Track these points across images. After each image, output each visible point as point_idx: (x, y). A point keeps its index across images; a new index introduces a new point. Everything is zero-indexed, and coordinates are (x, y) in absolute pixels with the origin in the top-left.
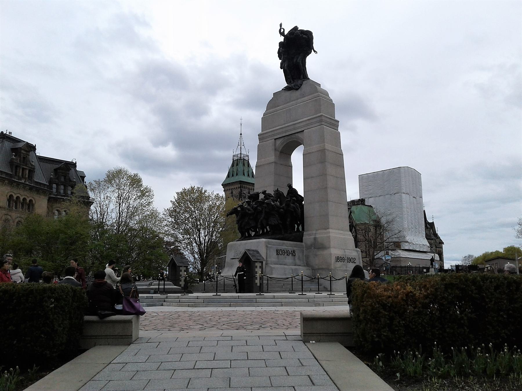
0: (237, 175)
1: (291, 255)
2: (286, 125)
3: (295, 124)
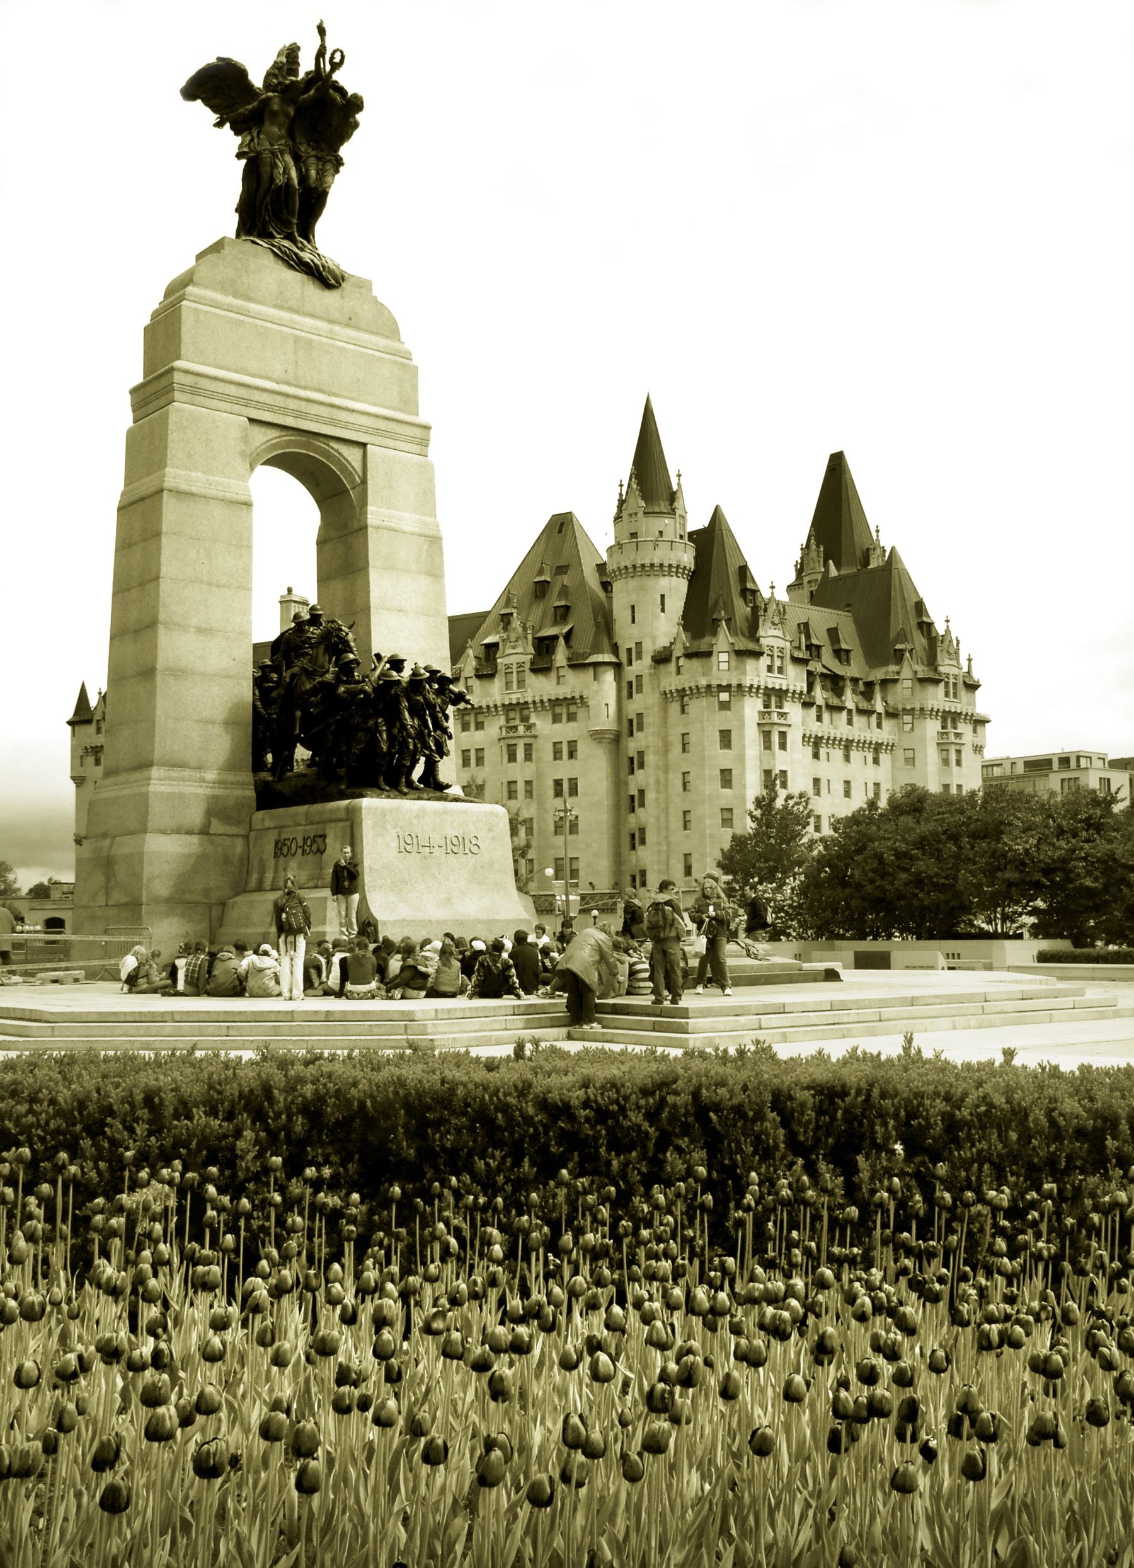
3: (339, 408)
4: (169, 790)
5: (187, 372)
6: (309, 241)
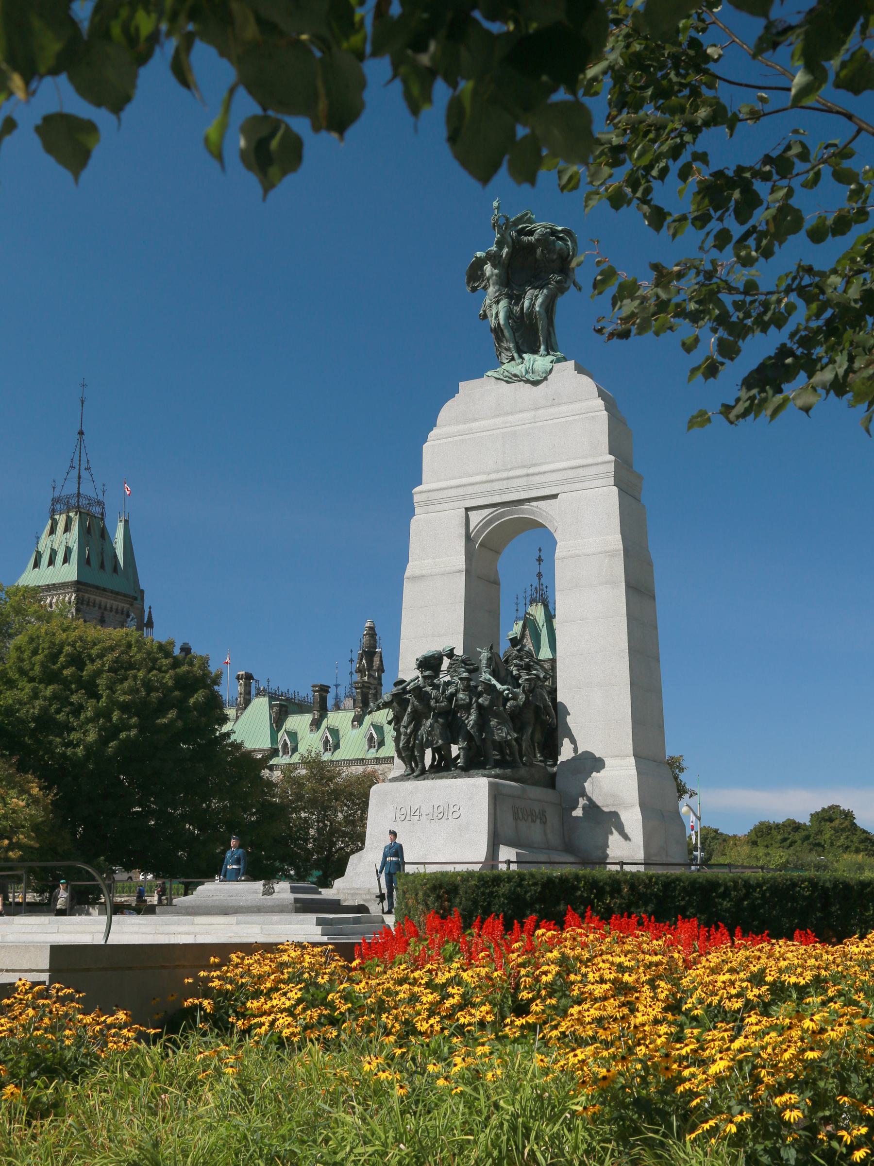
0: (66, 560)
1: (538, 821)
2: (504, 475)
3: (533, 474)
5: (421, 492)
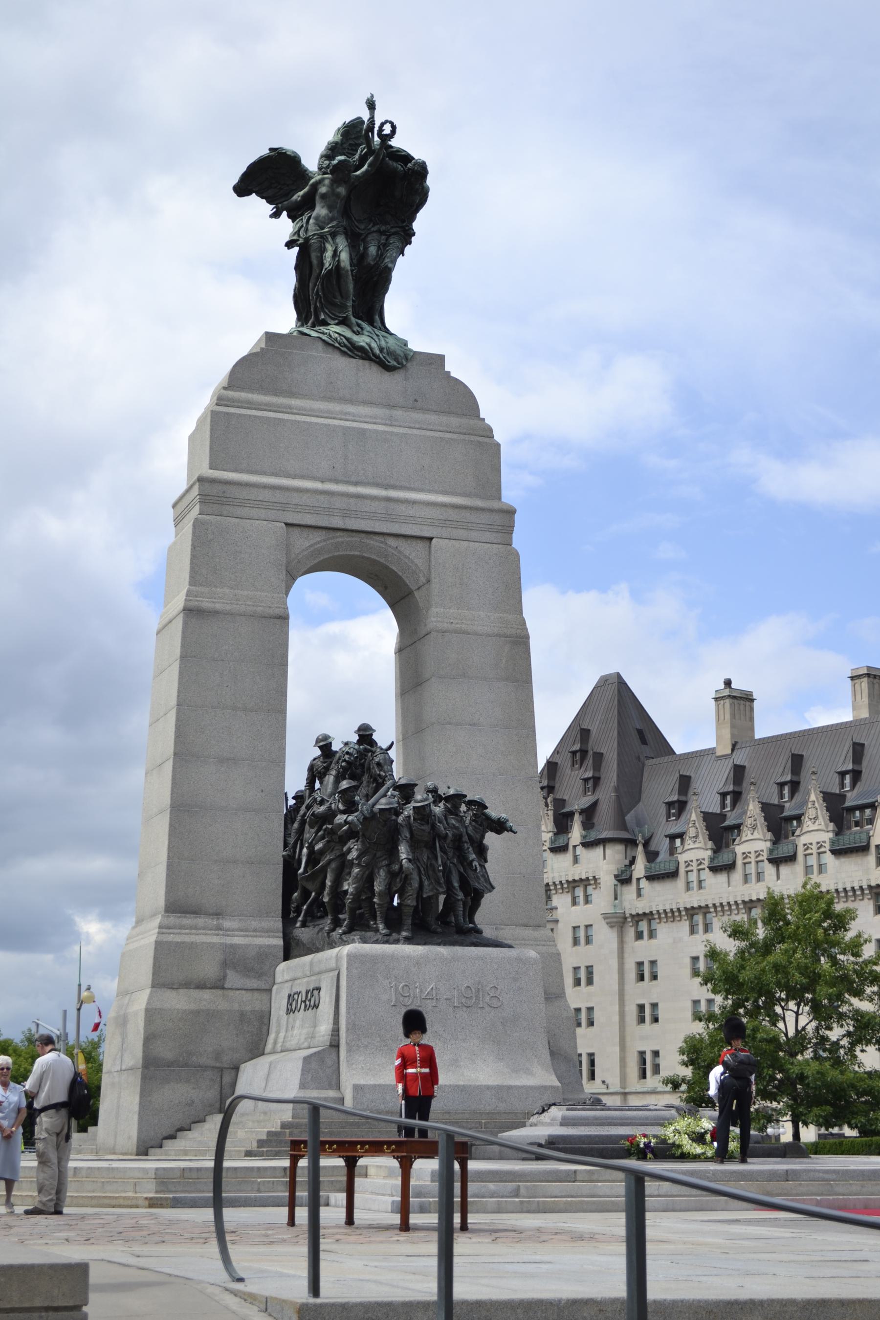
2: (352, 489)
4: (178, 939)
6: (371, 323)
